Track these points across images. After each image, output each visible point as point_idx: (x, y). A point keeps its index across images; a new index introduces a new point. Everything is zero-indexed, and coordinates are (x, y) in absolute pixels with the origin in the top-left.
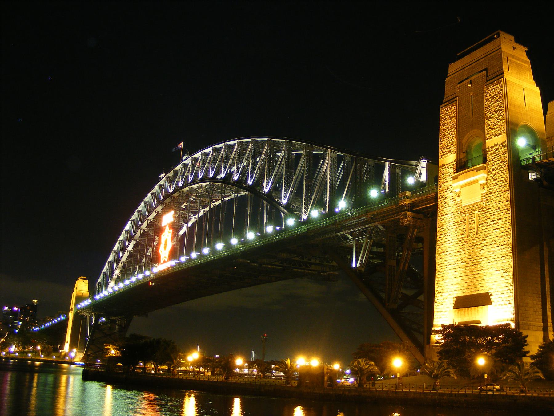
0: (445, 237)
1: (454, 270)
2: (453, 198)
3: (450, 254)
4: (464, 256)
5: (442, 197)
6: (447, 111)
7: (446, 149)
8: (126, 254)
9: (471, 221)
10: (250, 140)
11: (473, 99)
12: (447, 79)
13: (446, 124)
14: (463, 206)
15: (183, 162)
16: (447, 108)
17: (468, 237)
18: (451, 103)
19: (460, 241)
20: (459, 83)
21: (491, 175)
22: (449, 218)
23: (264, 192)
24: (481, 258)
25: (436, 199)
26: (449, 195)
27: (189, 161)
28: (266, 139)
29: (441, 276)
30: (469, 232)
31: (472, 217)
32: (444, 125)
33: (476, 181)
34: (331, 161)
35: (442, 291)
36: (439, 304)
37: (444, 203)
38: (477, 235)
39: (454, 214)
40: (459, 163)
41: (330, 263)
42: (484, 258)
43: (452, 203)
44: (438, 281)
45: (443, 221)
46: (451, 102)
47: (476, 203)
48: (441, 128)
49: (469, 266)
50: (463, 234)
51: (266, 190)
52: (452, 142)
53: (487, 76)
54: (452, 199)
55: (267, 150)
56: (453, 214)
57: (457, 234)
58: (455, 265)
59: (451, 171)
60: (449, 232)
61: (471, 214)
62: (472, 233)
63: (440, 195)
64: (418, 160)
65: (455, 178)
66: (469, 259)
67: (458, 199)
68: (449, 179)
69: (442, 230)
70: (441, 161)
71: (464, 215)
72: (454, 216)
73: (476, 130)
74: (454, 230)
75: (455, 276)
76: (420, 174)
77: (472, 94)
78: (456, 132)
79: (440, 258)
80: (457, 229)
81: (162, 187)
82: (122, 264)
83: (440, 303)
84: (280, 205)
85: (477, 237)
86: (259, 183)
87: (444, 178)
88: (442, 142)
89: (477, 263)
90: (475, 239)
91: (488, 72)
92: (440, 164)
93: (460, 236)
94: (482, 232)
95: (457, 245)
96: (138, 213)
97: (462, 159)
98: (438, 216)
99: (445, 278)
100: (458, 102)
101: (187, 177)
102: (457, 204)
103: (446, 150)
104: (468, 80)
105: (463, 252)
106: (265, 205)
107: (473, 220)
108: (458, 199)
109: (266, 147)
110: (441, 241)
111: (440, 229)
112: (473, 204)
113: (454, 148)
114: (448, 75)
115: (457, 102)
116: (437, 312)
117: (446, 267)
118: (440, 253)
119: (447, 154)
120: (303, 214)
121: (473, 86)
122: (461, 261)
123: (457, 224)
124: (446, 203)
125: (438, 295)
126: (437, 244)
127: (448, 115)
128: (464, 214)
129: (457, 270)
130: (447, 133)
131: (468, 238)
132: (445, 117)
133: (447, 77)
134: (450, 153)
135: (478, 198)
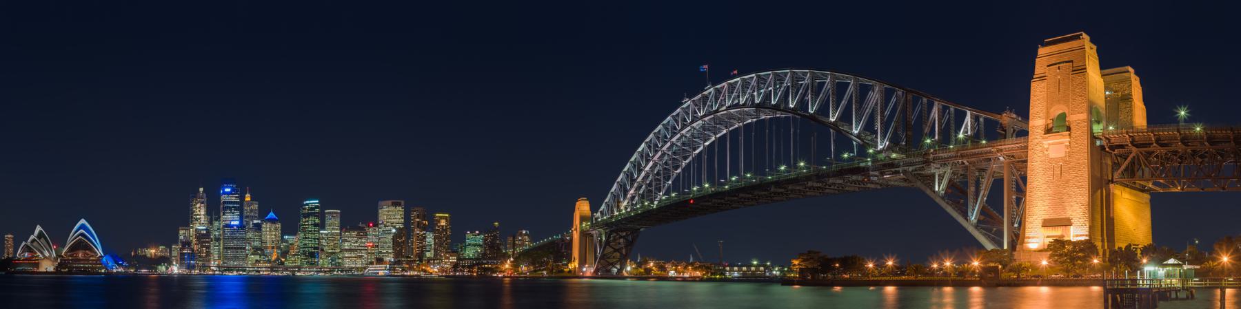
20: (1048, 66)
33: (1062, 143)
67: (1045, 152)
84: (851, 134)
86: (803, 104)
135: (1062, 155)
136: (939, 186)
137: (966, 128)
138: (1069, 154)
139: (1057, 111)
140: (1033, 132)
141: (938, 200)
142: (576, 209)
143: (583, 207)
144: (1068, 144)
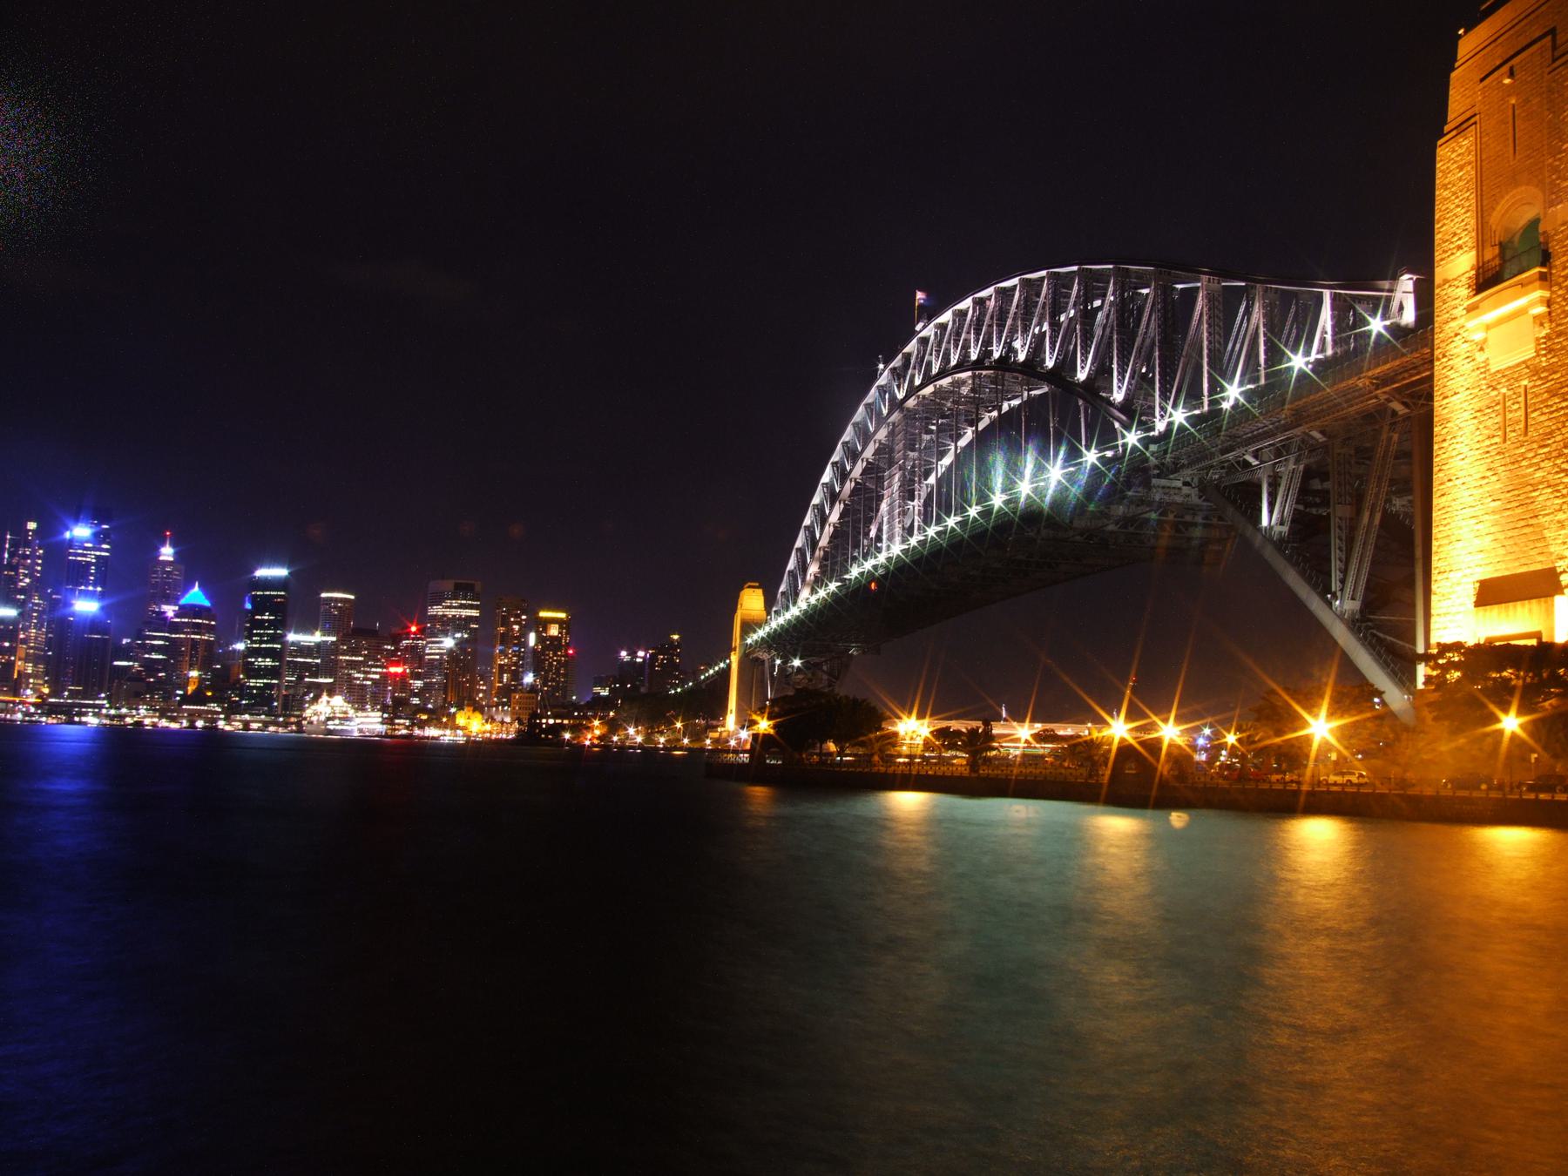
0: (1453, 446)
1: (1475, 521)
2: (1468, 354)
3: (1463, 483)
4: (1497, 487)
5: (1444, 356)
6: (1454, 151)
7: (1452, 243)
8: (828, 530)
9: (1513, 404)
10: (1043, 273)
11: (1517, 112)
12: (1453, 75)
13: (1449, 183)
14: (1493, 371)
15: (920, 335)
16: (1454, 145)
17: (1505, 441)
18: (1463, 131)
19: (1488, 452)
20: (1482, 80)
21: (1560, 292)
22: (1461, 403)
23: (1078, 380)
24: (1537, 489)
25: (1431, 362)
26: (1458, 348)
27: (929, 331)
28: (1075, 268)
29: (1445, 534)
30: (1508, 430)
31: (1514, 396)
32: (1445, 187)
33: (1521, 312)
34: (1209, 301)
35: (1448, 569)
36: (1442, 598)
37: (1449, 368)
38: (1526, 434)
39: (1472, 391)
40: (1484, 272)
41: (1211, 520)
42: (1543, 488)
43: (1466, 367)
44: (1439, 546)
45: (1446, 411)
46: (1461, 129)
47: (1524, 362)
48: (1438, 196)
49: (1509, 509)
50: (1494, 436)
51: (1082, 375)
52: (1466, 225)
53: (1554, 48)
54: (1468, 357)
55: (1079, 290)
56: (1469, 392)
57: (1480, 438)
58: (1476, 508)
59: (1463, 292)
60: (1460, 434)
61: (1512, 389)
62: (1514, 431)
63: (1439, 351)
64: (1395, 278)
65: (1471, 309)
66: (1508, 492)
67: (1480, 357)
68: (1459, 311)
69: (1445, 430)
70: (1440, 274)
71: (1495, 393)
72: (1472, 396)
73: (1523, 188)
74: (1474, 428)
75: (1478, 534)
76: (1401, 308)
77: (1513, 101)
78: (1474, 201)
79: (1443, 495)
80: (1481, 426)
81: (882, 390)
82: (822, 553)
83: (1443, 595)
84: (1112, 404)
85: (1527, 441)
87: (1448, 312)
88: (1442, 226)
89: (1529, 501)
90: (1522, 446)
91: (1558, 37)
92: (1438, 280)
93: (1488, 442)
94: (1539, 427)
95: (1479, 463)
96: (843, 447)
97: (1488, 262)
98: (1435, 399)
99: (1453, 538)
100: (1478, 126)
101: (929, 364)
102: (1478, 369)
103: (1452, 246)
104: (1505, 68)
105: (1494, 478)
106: (1082, 409)
107: (1518, 403)
108: (1480, 357)
109: (1076, 287)
110: (1444, 456)
111: (1440, 428)
112: (1518, 365)
113: (1468, 239)
114: (1457, 65)
115: (1476, 129)
116: (1438, 615)
117: (1455, 513)
118: (1441, 484)
119: (1453, 254)
120: (1156, 420)
121: (1518, 80)
122: (1490, 499)
123: (1478, 414)
124: (1452, 368)
125: (1440, 577)
126: (1435, 464)
127: (1455, 162)
128: (1494, 389)
129: (1481, 518)
130: (1453, 207)
131: (1506, 445)
132: (1448, 168)
133: (1454, 69)
134: (1461, 251)
135: (1528, 352)
136: (1271, 512)
137: (1323, 341)
138: (1548, 346)
139: (1519, 208)
140: (1444, 302)
141: (1269, 553)
142: (739, 606)
143: (751, 601)
144: (1542, 309)
